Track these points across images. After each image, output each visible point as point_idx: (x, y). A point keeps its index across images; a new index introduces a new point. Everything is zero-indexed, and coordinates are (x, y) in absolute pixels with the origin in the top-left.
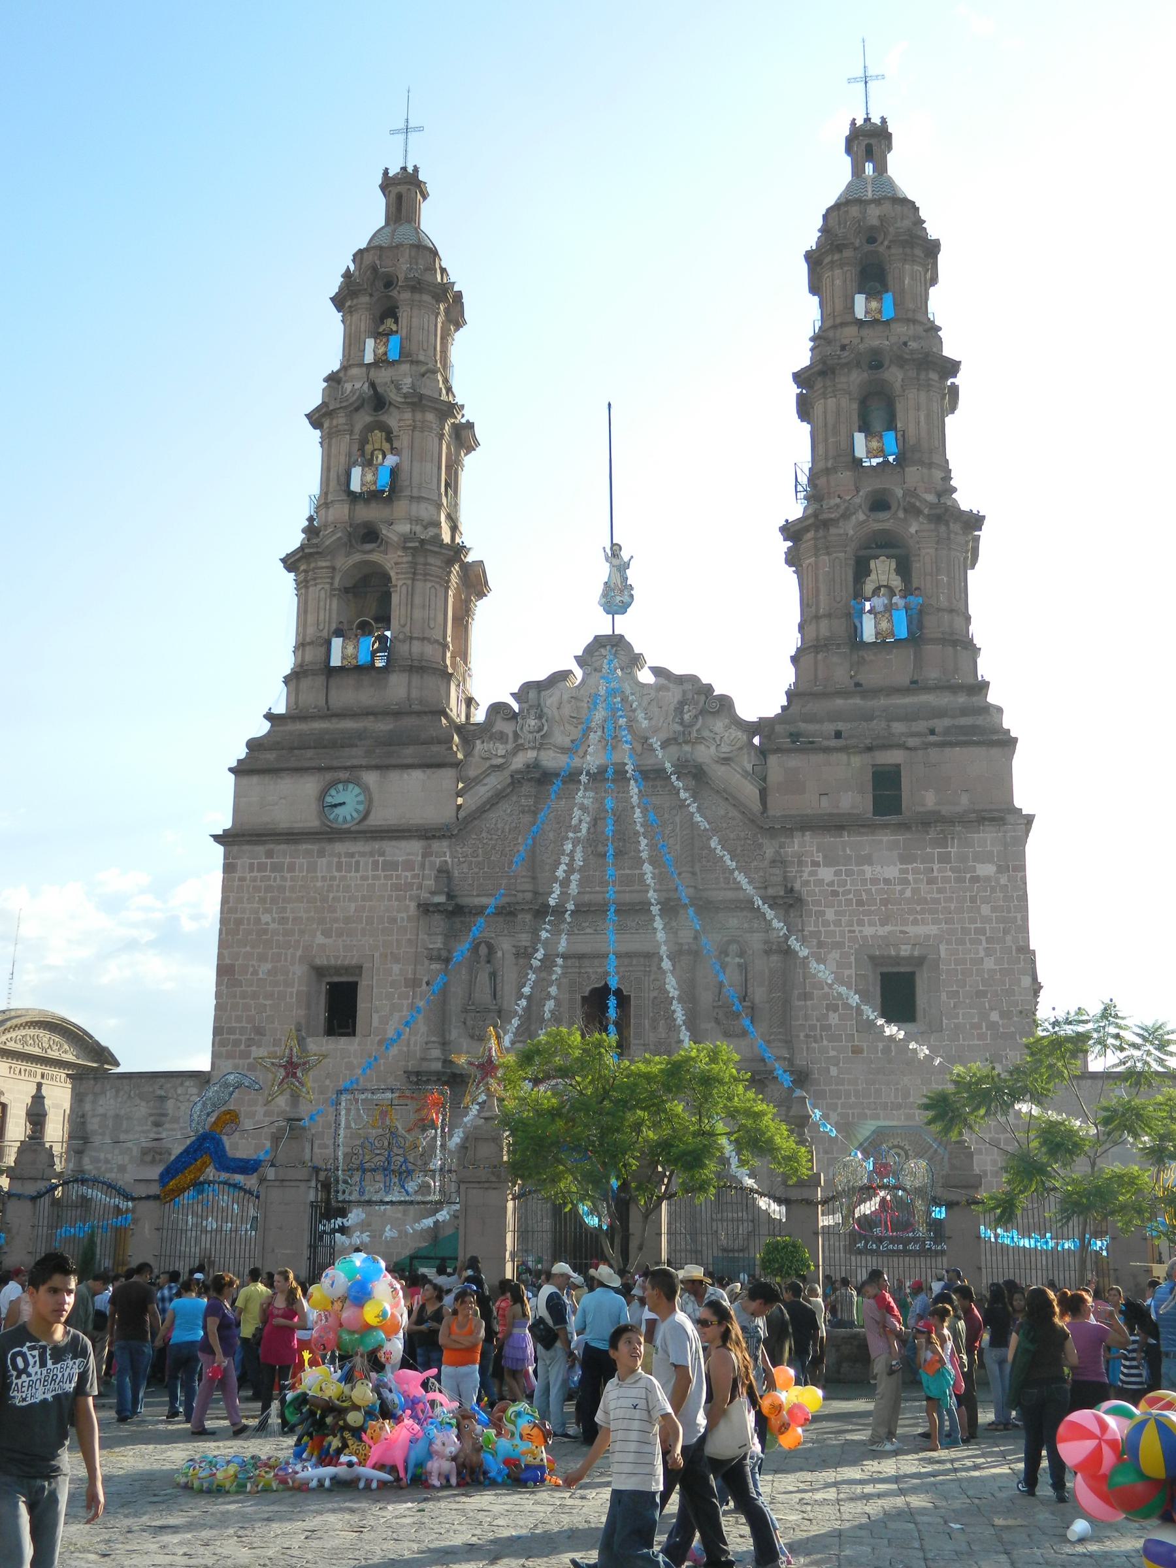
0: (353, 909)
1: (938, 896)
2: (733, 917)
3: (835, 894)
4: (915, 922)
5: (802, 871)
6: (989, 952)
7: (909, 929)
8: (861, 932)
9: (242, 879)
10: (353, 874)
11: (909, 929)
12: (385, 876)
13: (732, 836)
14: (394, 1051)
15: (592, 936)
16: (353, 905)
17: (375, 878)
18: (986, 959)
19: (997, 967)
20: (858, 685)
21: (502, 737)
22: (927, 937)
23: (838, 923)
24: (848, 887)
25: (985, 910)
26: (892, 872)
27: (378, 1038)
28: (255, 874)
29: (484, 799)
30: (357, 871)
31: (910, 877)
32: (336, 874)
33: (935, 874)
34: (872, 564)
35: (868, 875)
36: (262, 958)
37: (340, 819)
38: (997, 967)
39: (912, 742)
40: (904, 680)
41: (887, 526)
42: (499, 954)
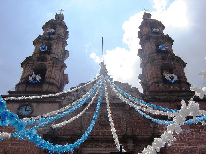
1: (203, 137)
2: (143, 144)
4: (198, 145)
7: (197, 146)
11: (197, 146)
15: (100, 148)
21: (73, 96)
22: (203, 149)
31: (194, 132)
33: (201, 131)
41: (167, 62)
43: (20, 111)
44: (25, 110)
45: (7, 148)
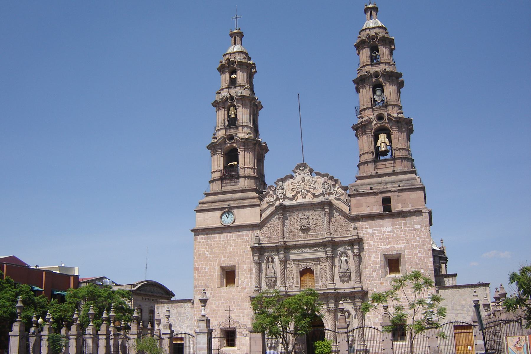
0: (232, 249)
3: (373, 236)
4: (397, 244)
5: (363, 230)
6: (420, 251)
7: (396, 246)
8: (381, 247)
9: (199, 242)
10: (231, 239)
11: (396, 246)
12: (241, 239)
13: (341, 221)
14: (246, 290)
16: (232, 248)
17: (238, 240)
18: (419, 253)
19: (422, 256)
20: (377, 173)
22: (401, 248)
23: (374, 245)
24: (377, 234)
25: (418, 239)
26: (390, 229)
27: (241, 287)
28: (203, 240)
29: (268, 214)
30: (232, 238)
31: (395, 230)
32: (226, 239)
34: (379, 136)
35: (382, 231)
36: (206, 265)
37: (227, 223)
38: (422, 256)
39: (393, 189)
40: (390, 170)
42: (275, 260)
43: (223, 220)
44: (228, 218)
45: (220, 261)
